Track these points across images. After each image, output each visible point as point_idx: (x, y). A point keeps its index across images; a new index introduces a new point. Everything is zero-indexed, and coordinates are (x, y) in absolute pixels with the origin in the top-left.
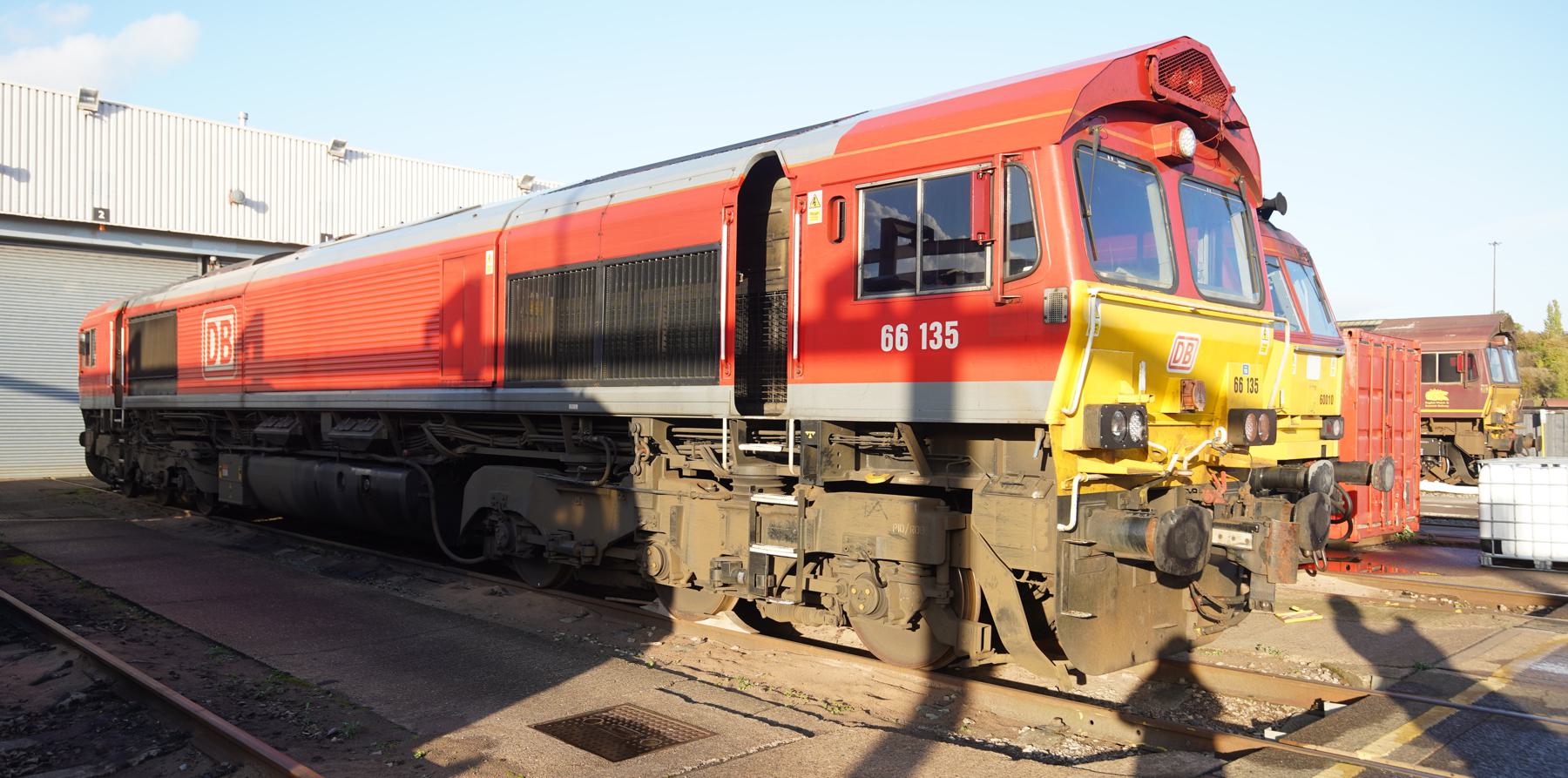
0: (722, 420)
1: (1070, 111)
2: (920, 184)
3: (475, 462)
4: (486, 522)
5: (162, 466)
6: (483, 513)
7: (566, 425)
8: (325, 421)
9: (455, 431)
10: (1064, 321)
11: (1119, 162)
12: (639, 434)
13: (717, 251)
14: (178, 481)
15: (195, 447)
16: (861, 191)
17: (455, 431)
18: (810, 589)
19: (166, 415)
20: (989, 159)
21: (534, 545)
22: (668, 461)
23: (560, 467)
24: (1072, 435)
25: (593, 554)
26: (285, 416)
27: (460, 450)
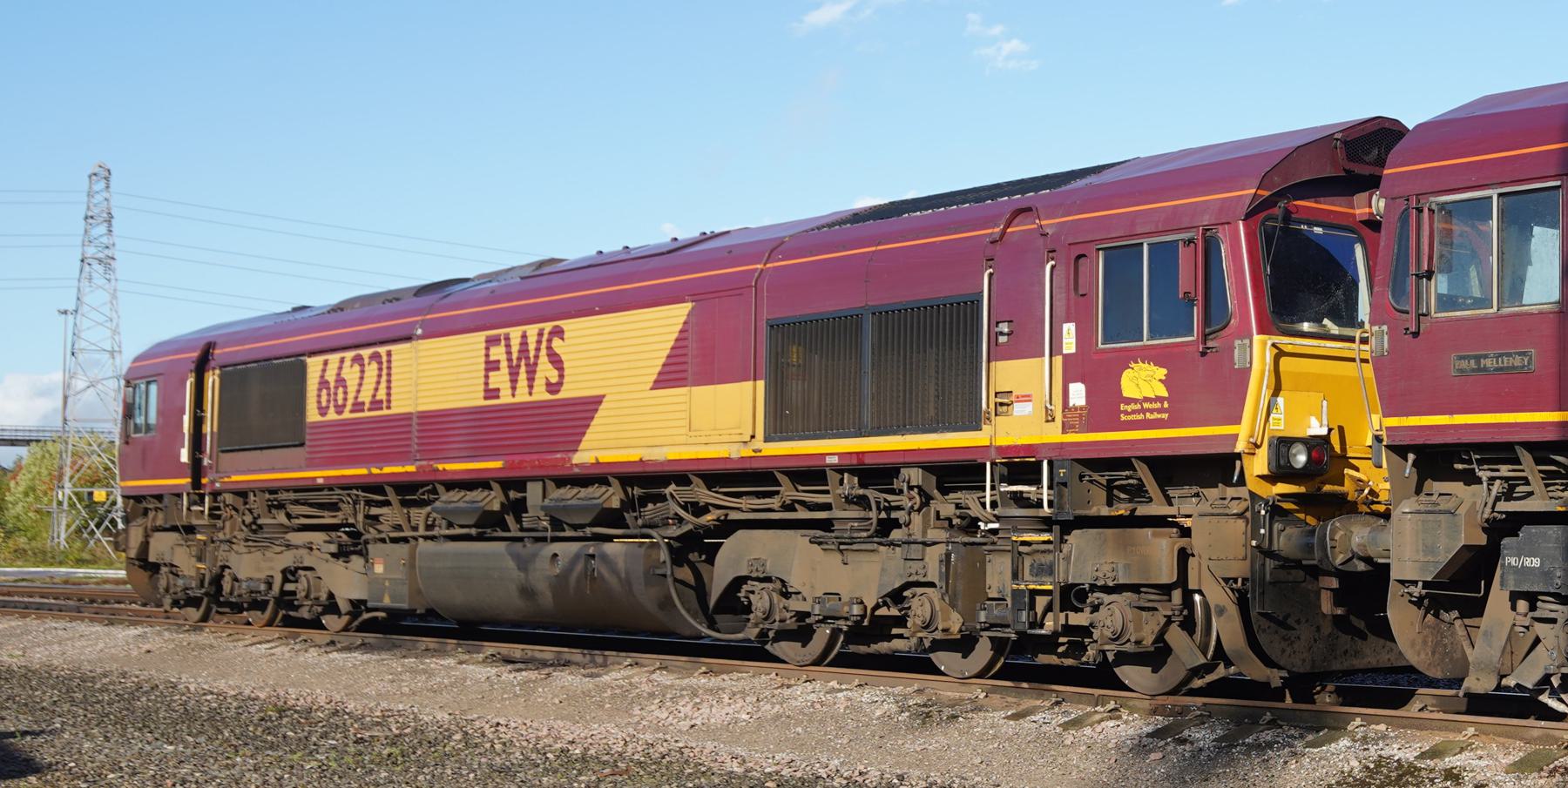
0: (985, 464)
1: (1253, 191)
2: (1145, 247)
3: (727, 528)
4: (742, 594)
5: (272, 569)
6: (739, 582)
7: (833, 477)
8: (533, 492)
9: (702, 494)
10: (1248, 365)
11: (1315, 228)
12: (909, 482)
13: (980, 302)
14: (300, 587)
15: (328, 538)
16: (1101, 252)
17: (702, 494)
18: (1070, 623)
19: (283, 496)
20: (1194, 230)
21: (797, 612)
22: (938, 513)
23: (826, 525)
24: (1258, 465)
25: (861, 613)
26: (477, 488)
27: (709, 517)
